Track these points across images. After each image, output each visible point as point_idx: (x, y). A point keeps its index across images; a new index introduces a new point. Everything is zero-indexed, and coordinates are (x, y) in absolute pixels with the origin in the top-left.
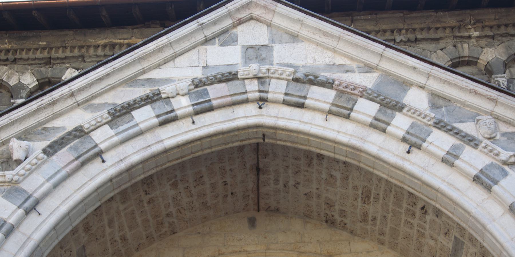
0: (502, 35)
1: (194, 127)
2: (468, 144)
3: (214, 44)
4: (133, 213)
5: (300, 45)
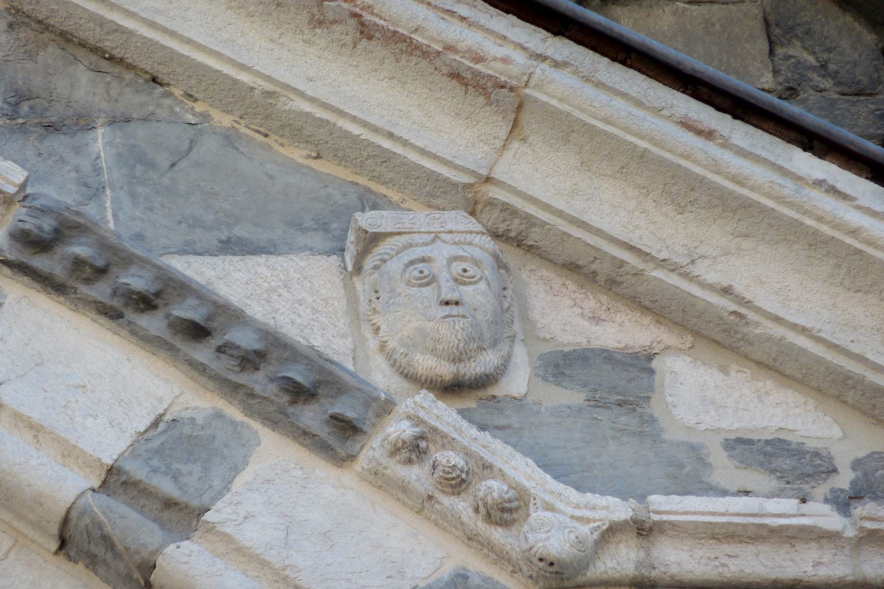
2: (277, 421)
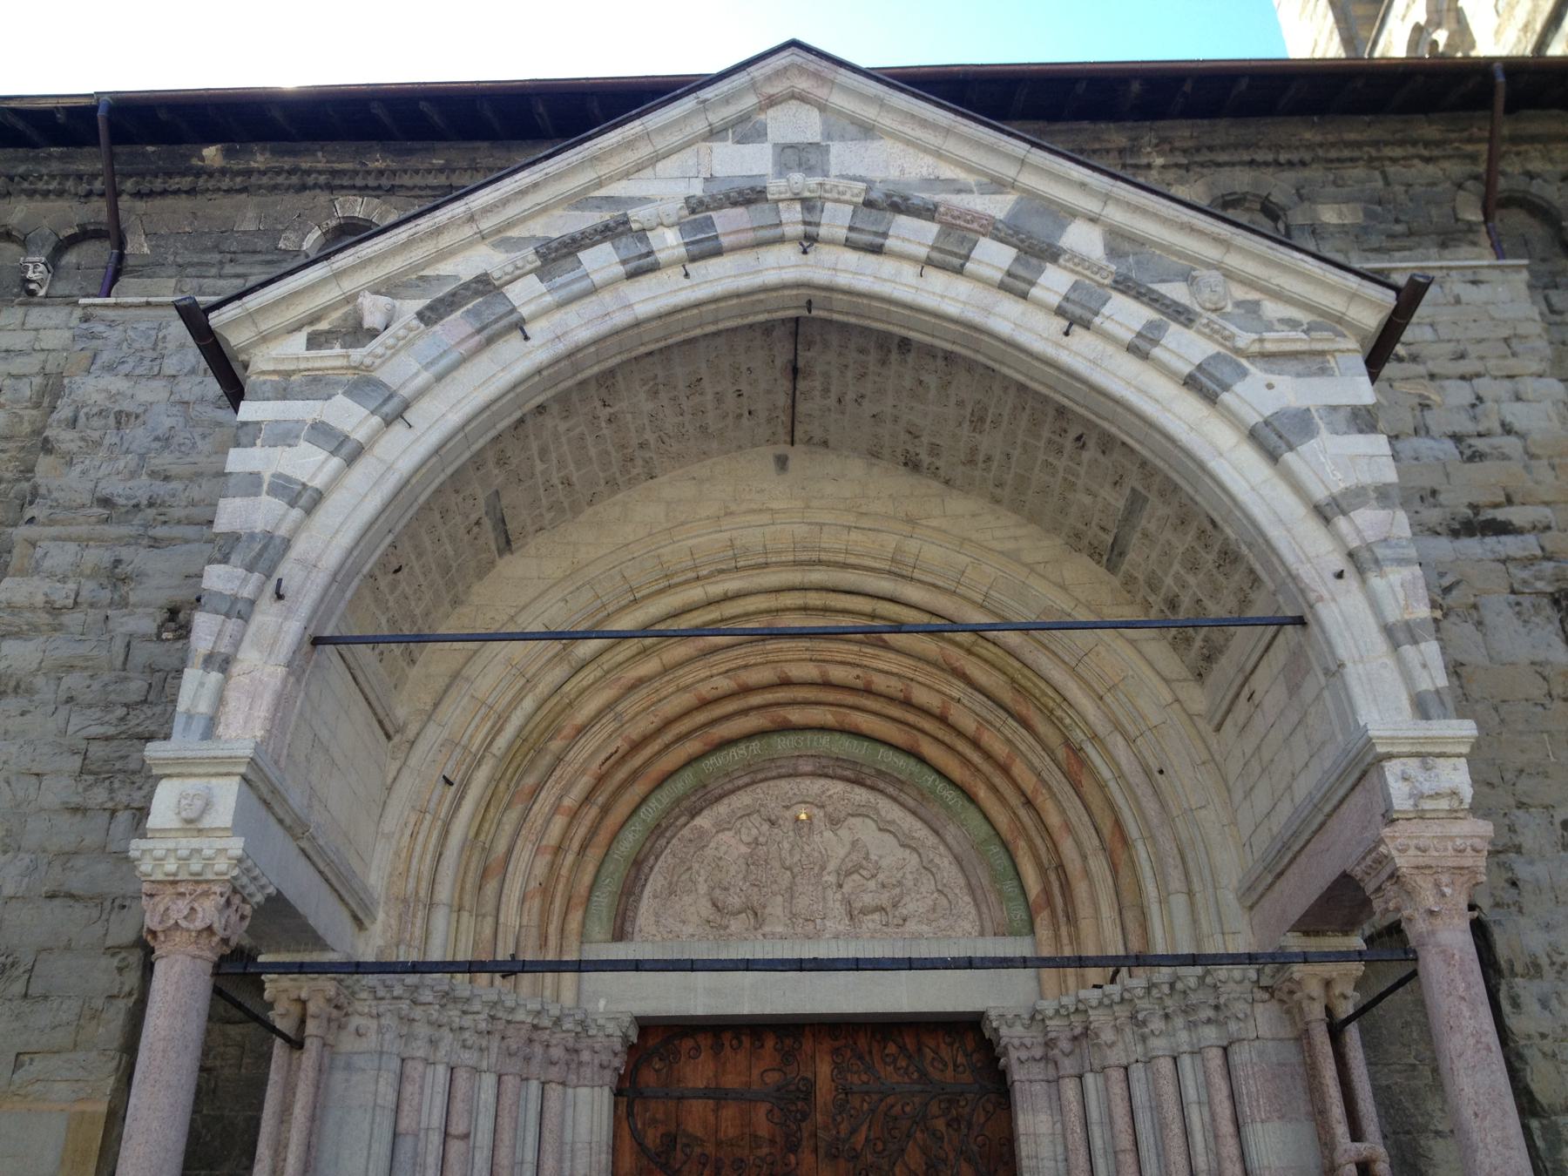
0: (1202, 165)
1: (687, 282)
2: (1175, 320)
3: (725, 139)
4: (582, 438)
5: (876, 144)
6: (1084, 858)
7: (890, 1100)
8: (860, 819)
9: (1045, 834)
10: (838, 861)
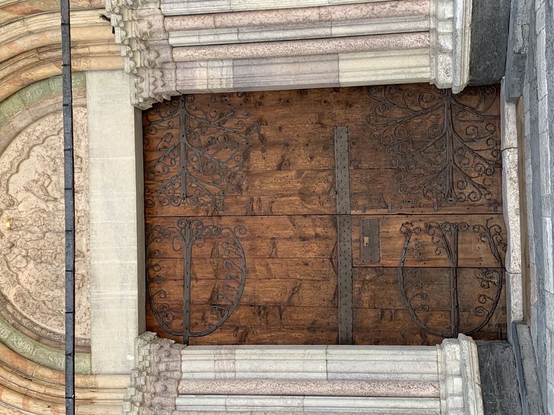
6: (31, 33)
7: (190, 169)
8: (10, 185)
9: (16, 59)
10: (39, 200)
